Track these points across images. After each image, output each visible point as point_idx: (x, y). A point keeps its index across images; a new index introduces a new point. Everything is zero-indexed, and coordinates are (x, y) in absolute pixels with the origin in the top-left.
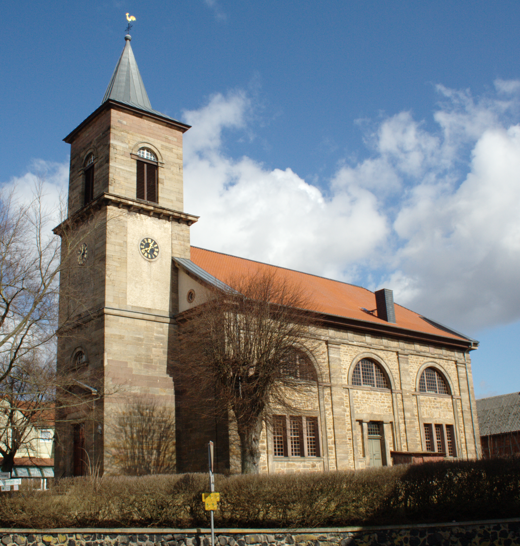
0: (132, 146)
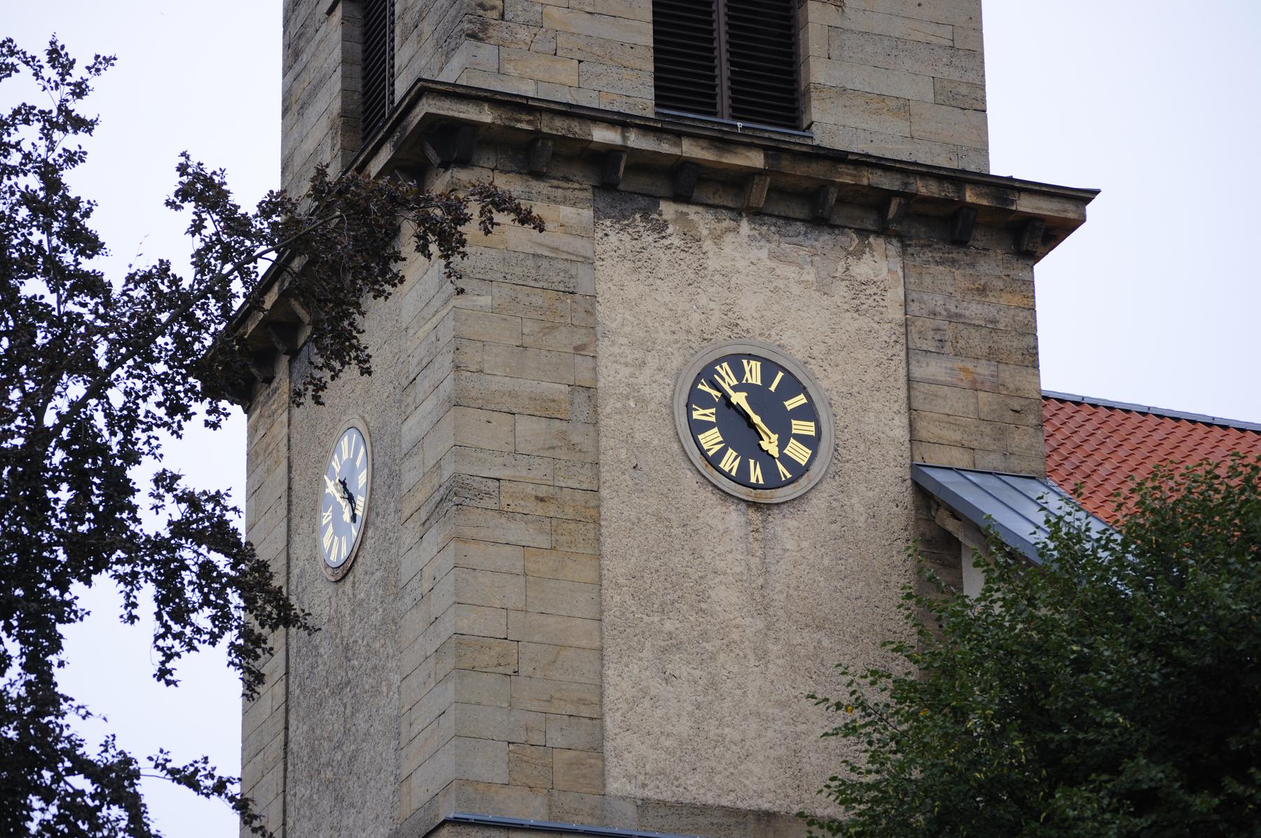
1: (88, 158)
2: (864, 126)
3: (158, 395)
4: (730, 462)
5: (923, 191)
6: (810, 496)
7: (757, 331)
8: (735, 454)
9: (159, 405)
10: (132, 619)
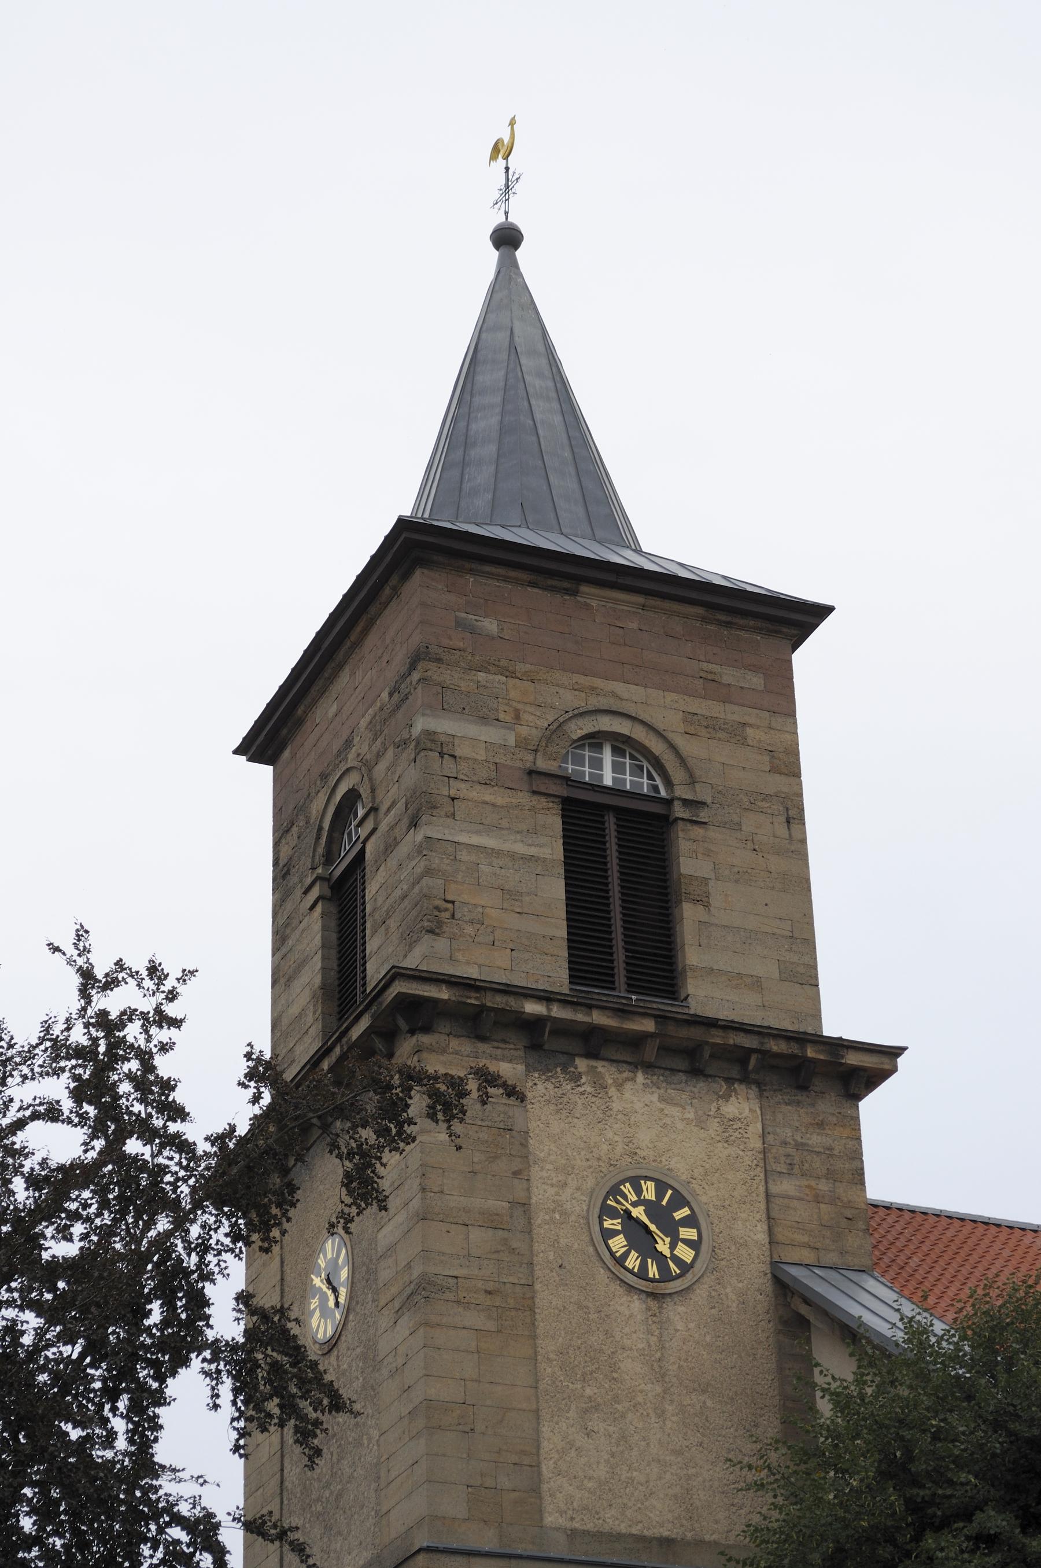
0: (536, 734)
1: (176, 1047)
2: (728, 998)
3: (225, 1228)
4: (633, 1261)
5: (775, 1049)
6: (695, 1287)
7: (652, 1158)
8: (636, 1255)
9: (226, 1235)
10: (216, 1407)
